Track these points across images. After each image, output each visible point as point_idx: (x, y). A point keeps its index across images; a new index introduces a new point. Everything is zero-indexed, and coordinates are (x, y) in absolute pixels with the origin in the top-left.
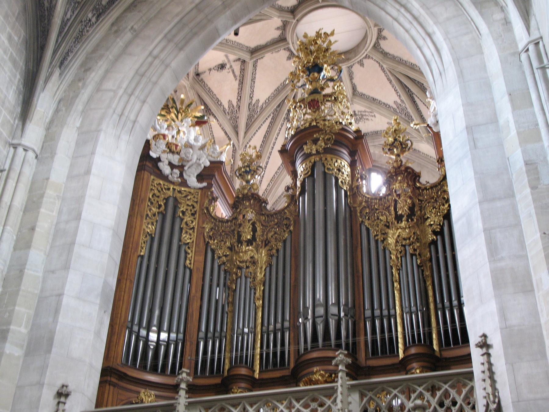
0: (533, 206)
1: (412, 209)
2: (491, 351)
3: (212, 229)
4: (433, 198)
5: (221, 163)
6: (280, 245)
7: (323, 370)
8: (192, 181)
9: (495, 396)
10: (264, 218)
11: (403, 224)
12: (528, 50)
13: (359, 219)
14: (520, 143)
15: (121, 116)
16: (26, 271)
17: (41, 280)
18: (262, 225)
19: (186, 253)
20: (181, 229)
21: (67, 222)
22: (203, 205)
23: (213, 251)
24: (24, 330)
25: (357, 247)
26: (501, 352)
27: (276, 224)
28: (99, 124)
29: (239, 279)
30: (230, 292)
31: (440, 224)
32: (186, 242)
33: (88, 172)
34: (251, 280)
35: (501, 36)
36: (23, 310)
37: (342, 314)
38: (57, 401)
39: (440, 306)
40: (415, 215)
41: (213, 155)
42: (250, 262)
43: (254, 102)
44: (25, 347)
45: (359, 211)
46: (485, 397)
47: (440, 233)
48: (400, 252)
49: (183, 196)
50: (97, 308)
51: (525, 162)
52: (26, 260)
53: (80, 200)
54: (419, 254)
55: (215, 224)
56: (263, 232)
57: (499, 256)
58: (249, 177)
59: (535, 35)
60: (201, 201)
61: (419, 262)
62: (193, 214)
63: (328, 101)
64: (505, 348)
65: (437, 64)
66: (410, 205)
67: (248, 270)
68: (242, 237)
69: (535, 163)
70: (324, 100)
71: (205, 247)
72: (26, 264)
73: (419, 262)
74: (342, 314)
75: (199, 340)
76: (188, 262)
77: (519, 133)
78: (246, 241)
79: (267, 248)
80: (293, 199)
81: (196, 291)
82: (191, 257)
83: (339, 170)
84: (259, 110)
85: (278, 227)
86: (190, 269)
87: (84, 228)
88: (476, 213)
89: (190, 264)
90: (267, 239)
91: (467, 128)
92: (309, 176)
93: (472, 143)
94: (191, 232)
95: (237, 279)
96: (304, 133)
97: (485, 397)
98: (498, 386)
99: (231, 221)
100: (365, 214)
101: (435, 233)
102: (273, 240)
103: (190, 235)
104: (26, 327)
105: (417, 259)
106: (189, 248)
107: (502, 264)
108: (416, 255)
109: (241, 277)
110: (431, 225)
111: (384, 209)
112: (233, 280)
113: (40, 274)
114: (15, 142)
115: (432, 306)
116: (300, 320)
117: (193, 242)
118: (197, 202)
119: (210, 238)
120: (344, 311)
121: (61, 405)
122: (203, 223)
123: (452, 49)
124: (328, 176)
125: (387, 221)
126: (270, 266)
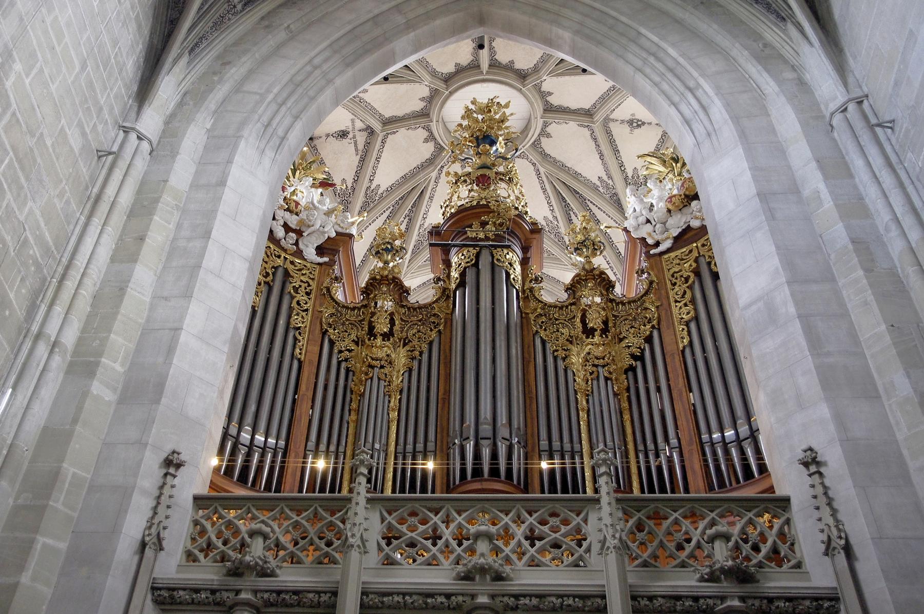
1: (605, 323)
3: (332, 315)
5: (351, 236)
6: (425, 347)
8: (310, 253)
11: (597, 339)
13: (532, 328)
19: (295, 339)
20: (291, 309)
23: (332, 343)
25: (529, 362)
27: (420, 321)
30: (353, 397)
32: (297, 326)
38: (164, 471)
39: (641, 447)
40: (609, 332)
41: (342, 225)
43: (373, 187)
47: (641, 358)
48: (591, 374)
49: (297, 268)
50: (224, 358)
54: (616, 379)
58: (389, 257)
60: (319, 278)
61: (616, 388)
62: (308, 294)
63: (501, 179)
66: (604, 319)
67: (382, 370)
70: (496, 178)
71: (321, 335)
75: (307, 452)
76: (298, 351)
78: (381, 335)
79: (407, 348)
80: (446, 295)
81: (307, 389)
82: (303, 345)
83: (511, 264)
84: (377, 198)
85: (423, 324)
86: (299, 360)
87: (212, 248)
89: (300, 354)
90: (407, 338)
92: (473, 265)
94: (304, 314)
95: (366, 380)
96: (470, 212)
99: (359, 309)
100: (540, 323)
101: (634, 357)
103: (303, 317)
105: (613, 384)
106: (300, 334)
108: (611, 379)
109: (372, 378)
110: (629, 347)
111: (565, 320)
115: (631, 446)
117: (305, 327)
118: (313, 279)
119: (330, 325)
121: (169, 477)
122: (321, 305)
123: (728, 106)
124: (497, 269)
125: (570, 336)
126: (410, 370)
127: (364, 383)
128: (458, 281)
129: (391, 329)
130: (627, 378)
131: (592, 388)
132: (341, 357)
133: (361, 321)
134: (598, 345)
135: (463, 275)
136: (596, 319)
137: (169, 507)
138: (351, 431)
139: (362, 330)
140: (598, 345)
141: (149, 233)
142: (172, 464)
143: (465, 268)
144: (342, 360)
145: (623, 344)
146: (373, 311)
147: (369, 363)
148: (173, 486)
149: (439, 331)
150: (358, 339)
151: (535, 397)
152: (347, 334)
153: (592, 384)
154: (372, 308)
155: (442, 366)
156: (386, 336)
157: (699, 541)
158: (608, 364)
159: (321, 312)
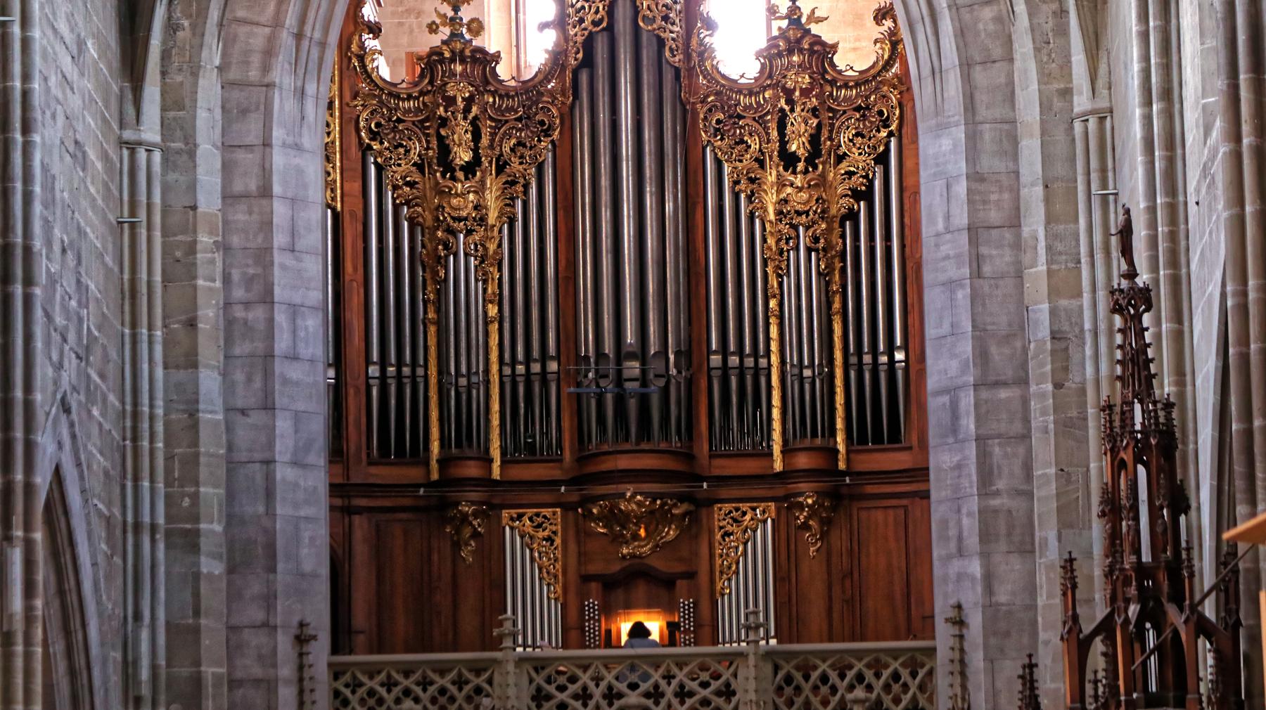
0: (1052, 418)
1: (815, 140)
2: (965, 631)
4: (858, 109)
7: (641, 494)
9: (963, 699)
10: (491, 100)
11: (798, 181)
12: (1087, 120)
14: (1049, 295)
15: (299, 36)
16: (201, 415)
17: (223, 427)
18: (491, 119)
21: (247, 305)
22: (349, 48)
23: (379, 169)
24: (218, 528)
26: (980, 640)
27: (519, 119)
28: (266, 68)
29: (452, 257)
31: (868, 175)
33: (265, 192)
34: (477, 262)
35: (1049, 43)
36: (211, 490)
37: (673, 371)
39: (853, 360)
40: (820, 156)
42: (474, 219)
44: (225, 557)
45: (702, 116)
46: (951, 698)
47: (866, 195)
51: (1052, 332)
52: (197, 393)
53: (263, 256)
54: (824, 249)
55: (381, 101)
56: (493, 135)
57: (994, 488)
59: (1104, 104)
64: (986, 637)
65: (928, 43)
68: (453, 154)
69: (1065, 338)
71: (360, 153)
72: (197, 402)
73: (823, 267)
74: (673, 371)
77: (1050, 273)
78: (462, 168)
79: (503, 178)
81: (355, 269)
82: (335, 181)
83: (666, 18)
85: (527, 127)
87: (281, 318)
88: (967, 400)
91: (969, 229)
92: (603, 29)
93: (975, 265)
97: (951, 698)
98: (970, 687)
101: (856, 195)
102: (518, 161)
104: (219, 522)
105: (818, 260)
107: (996, 502)
109: (456, 255)
110: (850, 174)
112: (440, 257)
113: (220, 417)
114: (128, 135)
116: (591, 375)
119: (374, 136)
120: (676, 366)
121: (304, 657)
122: (355, 97)
123: (961, 33)
125: (760, 150)
127: (443, 261)
128: (580, 56)
129: (476, 150)
130: (843, 236)
131: (788, 266)
132: (398, 198)
133: (422, 122)
134: (800, 189)
135: (589, 44)
136: (800, 136)
137: (312, 691)
138: (432, 342)
139: (428, 142)
140: (800, 189)
141: (200, 313)
142: (302, 639)
143: (591, 33)
144: (402, 204)
145: (844, 167)
146: (443, 114)
147: (448, 225)
148: (310, 666)
149: (553, 142)
150: (422, 160)
151: (703, 273)
152: (401, 150)
153: (788, 260)
154: (441, 109)
155: (561, 213)
156: (470, 169)
157: (843, 697)
158: (814, 223)
159: (356, 106)
